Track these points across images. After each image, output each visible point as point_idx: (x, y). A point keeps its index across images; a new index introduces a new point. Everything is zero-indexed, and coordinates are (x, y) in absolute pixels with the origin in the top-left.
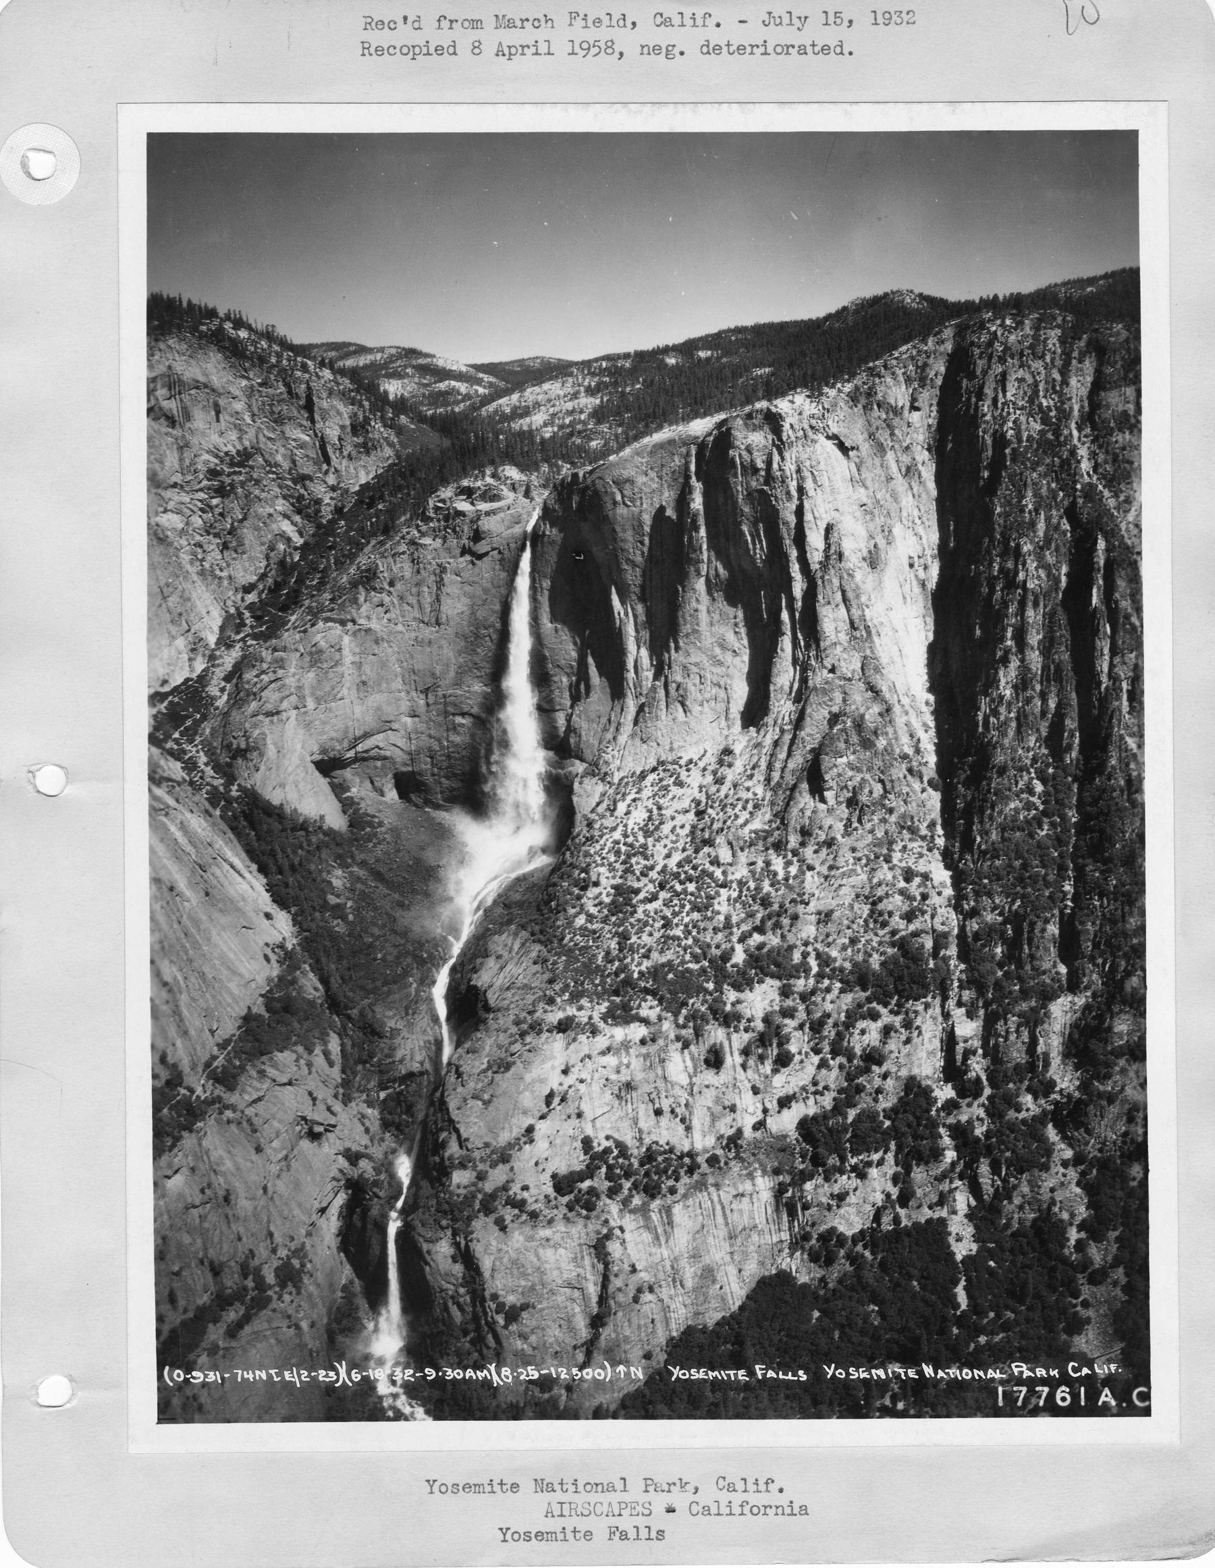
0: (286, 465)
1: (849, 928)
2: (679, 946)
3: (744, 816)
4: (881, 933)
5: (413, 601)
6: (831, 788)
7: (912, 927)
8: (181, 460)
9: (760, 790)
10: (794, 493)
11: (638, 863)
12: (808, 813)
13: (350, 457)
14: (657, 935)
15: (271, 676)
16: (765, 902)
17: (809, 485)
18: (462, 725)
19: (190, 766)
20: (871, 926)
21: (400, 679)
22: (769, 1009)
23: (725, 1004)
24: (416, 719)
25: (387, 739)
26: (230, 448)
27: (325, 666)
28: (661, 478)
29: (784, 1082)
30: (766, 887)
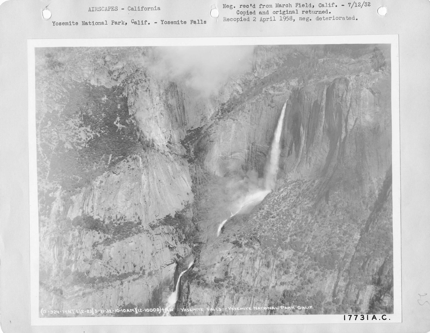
1: (319, 243)
2: (273, 232)
4: (328, 247)
6: (330, 200)
7: (338, 249)
11: (276, 207)
12: (323, 206)
13: (263, 69)
14: (269, 227)
16: (301, 228)
19: (188, 151)
20: (326, 244)
22: (288, 257)
23: (277, 251)
27: (227, 131)
29: (284, 278)
30: (303, 224)
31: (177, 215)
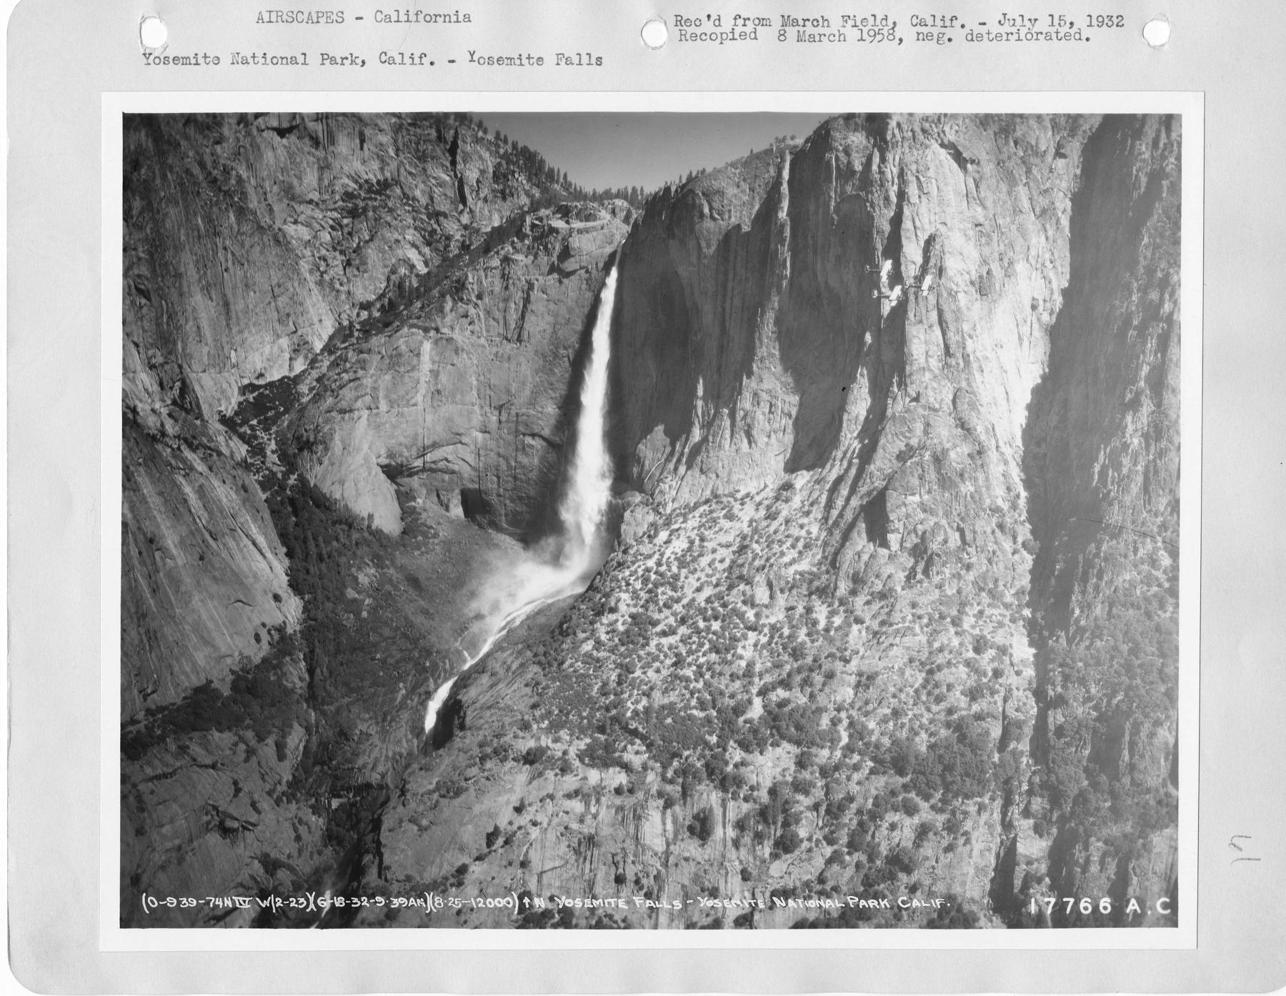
0: (424, 200)
1: (894, 696)
2: (686, 688)
3: (793, 554)
4: (935, 708)
5: (499, 315)
6: (897, 530)
7: (975, 708)
8: (320, 179)
9: (815, 529)
10: (894, 199)
11: (664, 593)
12: (865, 557)
13: (485, 200)
14: (665, 672)
15: (351, 375)
16: (797, 653)
17: (912, 190)
18: (531, 446)
20: (924, 698)
21: (475, 392)
22: (779, 778)
23: (727, 763)
24: (487, 435)
25: (456, 452)
26: (371, 176)
27: (402, 369)
28: (752, 190)
30: (802, 635)
31: (242, 684)
